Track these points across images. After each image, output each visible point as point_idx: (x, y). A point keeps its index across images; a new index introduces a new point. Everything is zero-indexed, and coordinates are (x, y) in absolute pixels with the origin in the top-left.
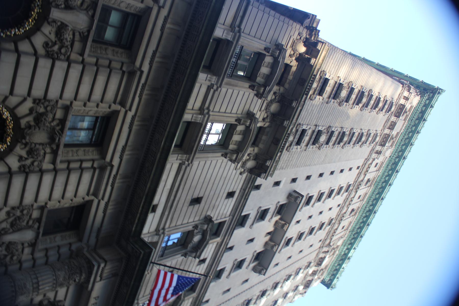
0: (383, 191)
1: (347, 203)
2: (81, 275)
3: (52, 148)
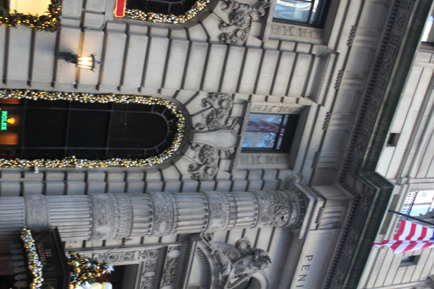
2: (291, 212)
3: (260, 14)
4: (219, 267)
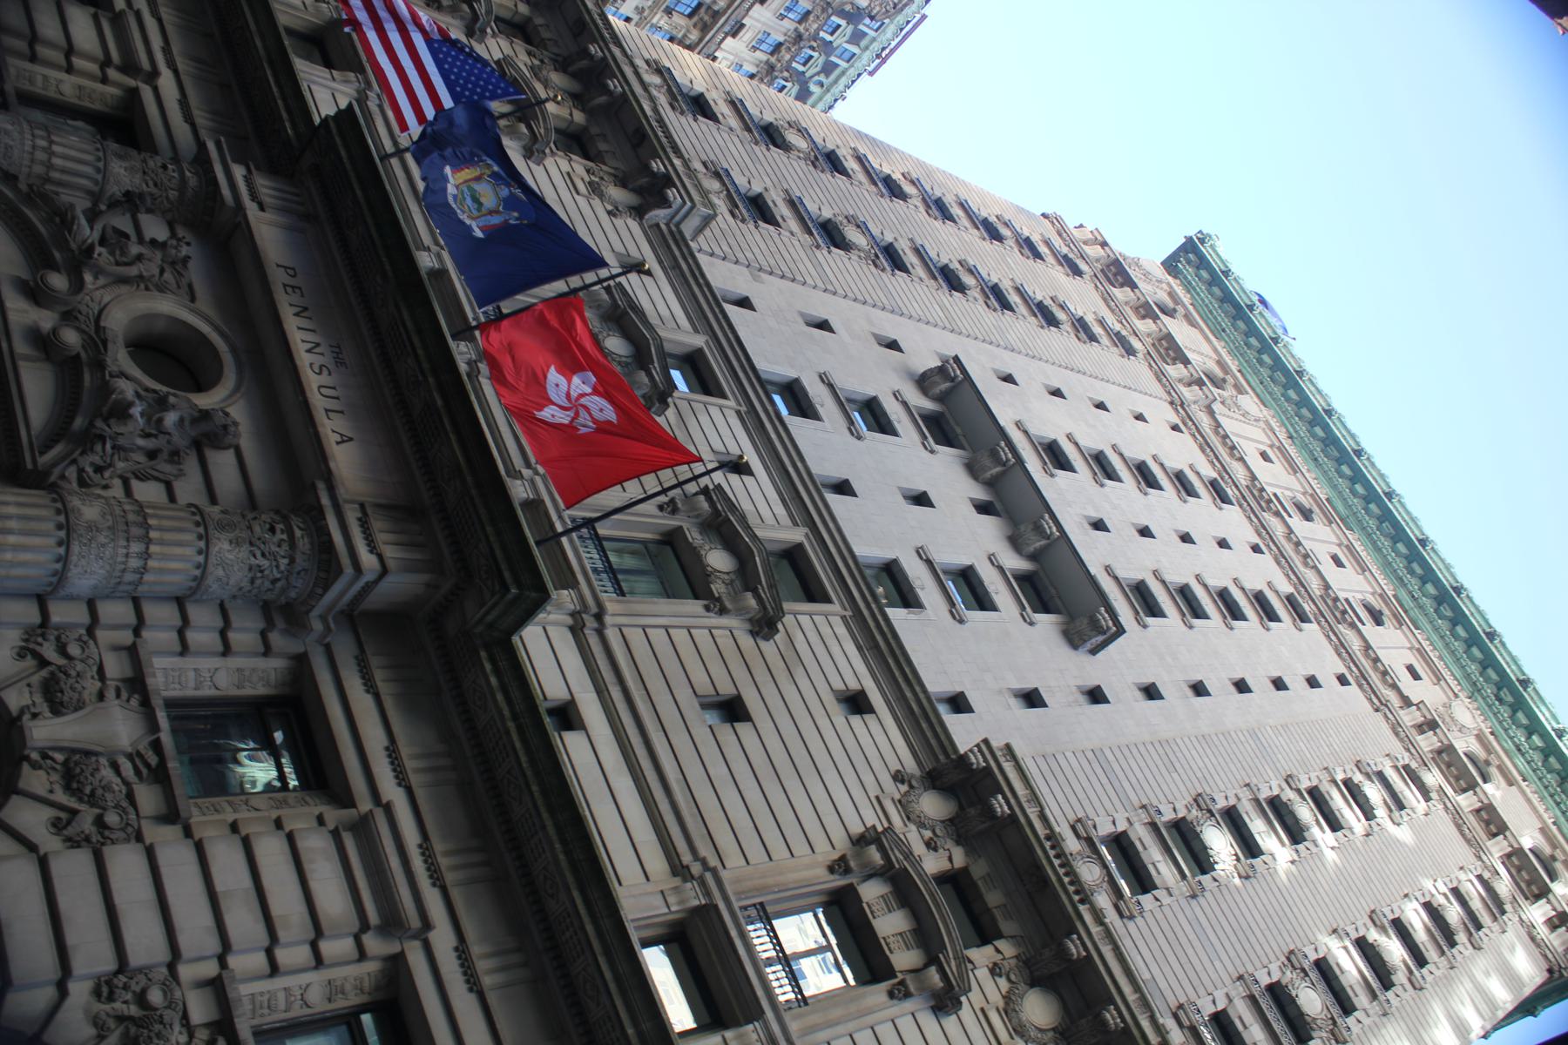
0: (1396, 524)
1: (1297, 561)
4: (57, 220)
